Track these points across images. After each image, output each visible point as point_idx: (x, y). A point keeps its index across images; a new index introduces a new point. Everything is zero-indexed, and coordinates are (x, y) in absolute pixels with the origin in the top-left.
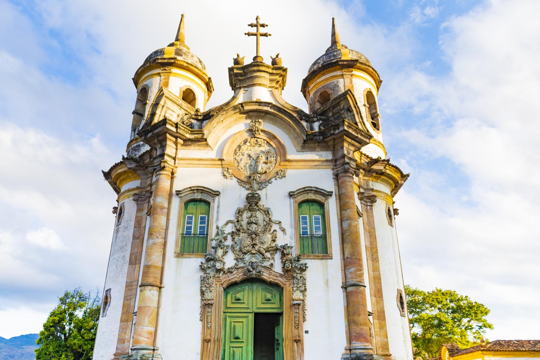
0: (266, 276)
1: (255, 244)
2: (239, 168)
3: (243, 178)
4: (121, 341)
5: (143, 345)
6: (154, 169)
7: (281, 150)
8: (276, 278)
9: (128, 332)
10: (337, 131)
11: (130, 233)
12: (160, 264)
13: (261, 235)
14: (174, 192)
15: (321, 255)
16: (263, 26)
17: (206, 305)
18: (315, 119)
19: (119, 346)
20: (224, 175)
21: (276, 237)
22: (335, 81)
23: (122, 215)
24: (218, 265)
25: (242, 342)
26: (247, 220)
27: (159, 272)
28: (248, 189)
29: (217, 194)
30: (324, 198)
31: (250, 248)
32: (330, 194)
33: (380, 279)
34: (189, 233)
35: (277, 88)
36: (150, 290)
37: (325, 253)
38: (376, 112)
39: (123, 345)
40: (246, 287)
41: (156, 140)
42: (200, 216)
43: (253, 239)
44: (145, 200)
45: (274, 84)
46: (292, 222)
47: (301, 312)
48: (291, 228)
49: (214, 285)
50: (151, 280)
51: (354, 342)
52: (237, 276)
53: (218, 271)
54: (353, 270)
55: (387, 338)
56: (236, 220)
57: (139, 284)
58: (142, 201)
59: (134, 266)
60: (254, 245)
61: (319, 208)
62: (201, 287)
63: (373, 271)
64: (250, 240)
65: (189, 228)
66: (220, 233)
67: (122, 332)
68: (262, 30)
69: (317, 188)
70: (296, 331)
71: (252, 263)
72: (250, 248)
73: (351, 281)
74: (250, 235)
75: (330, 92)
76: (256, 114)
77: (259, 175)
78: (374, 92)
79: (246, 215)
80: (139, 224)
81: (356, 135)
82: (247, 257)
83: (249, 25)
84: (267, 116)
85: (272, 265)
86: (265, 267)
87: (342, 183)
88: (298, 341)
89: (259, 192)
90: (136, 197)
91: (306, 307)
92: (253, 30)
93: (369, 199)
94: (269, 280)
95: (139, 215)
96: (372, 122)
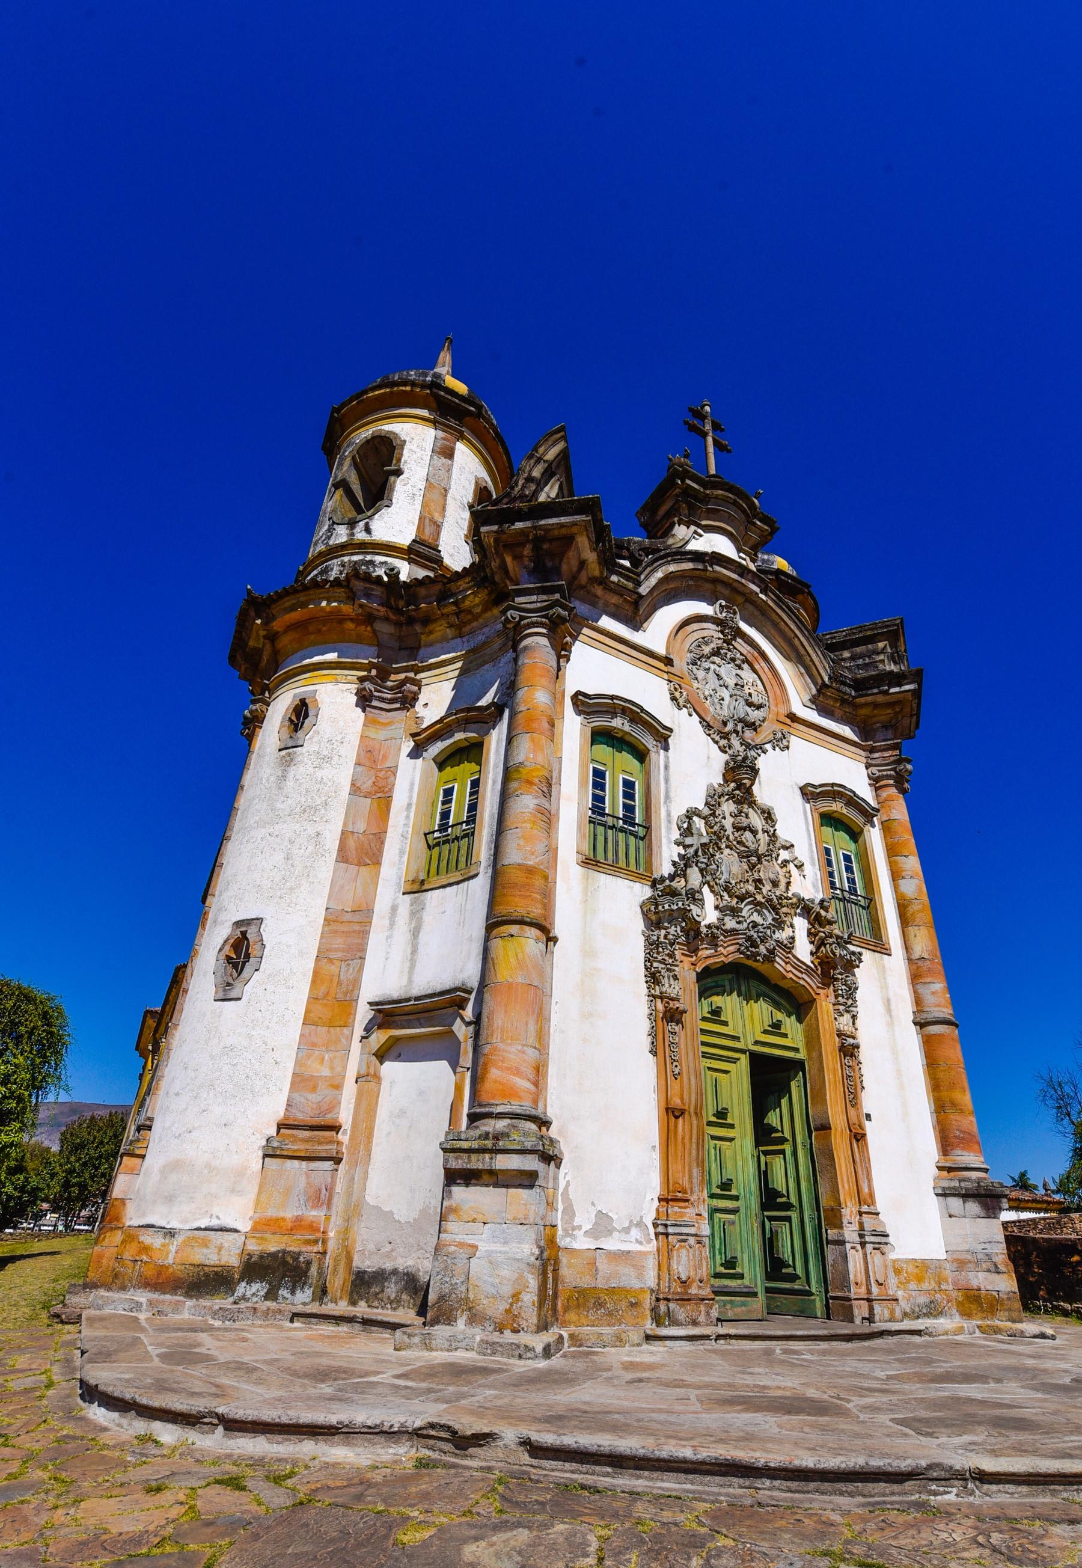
1: (760, 881)
6: (522, 618)
7: (777, 689)
8: (799, 974)
10: (892, 690)
11: (342, 774)
20: (674, 699)
25: (732, 1126)
26: (732, 820)
31: (751, 888)
39: (310, 1096)
41: (527, 551)
43: (752, 867)
44: (392, 701)
47: (857, 1068)
48: (813, 864)
51: (959, 1152)
59: (353, 869)
62: (649, 960)
67: (309, 1056)
72: (751, 888)
84: (747, 605)
90: (368, 685)
95: (372, 735)
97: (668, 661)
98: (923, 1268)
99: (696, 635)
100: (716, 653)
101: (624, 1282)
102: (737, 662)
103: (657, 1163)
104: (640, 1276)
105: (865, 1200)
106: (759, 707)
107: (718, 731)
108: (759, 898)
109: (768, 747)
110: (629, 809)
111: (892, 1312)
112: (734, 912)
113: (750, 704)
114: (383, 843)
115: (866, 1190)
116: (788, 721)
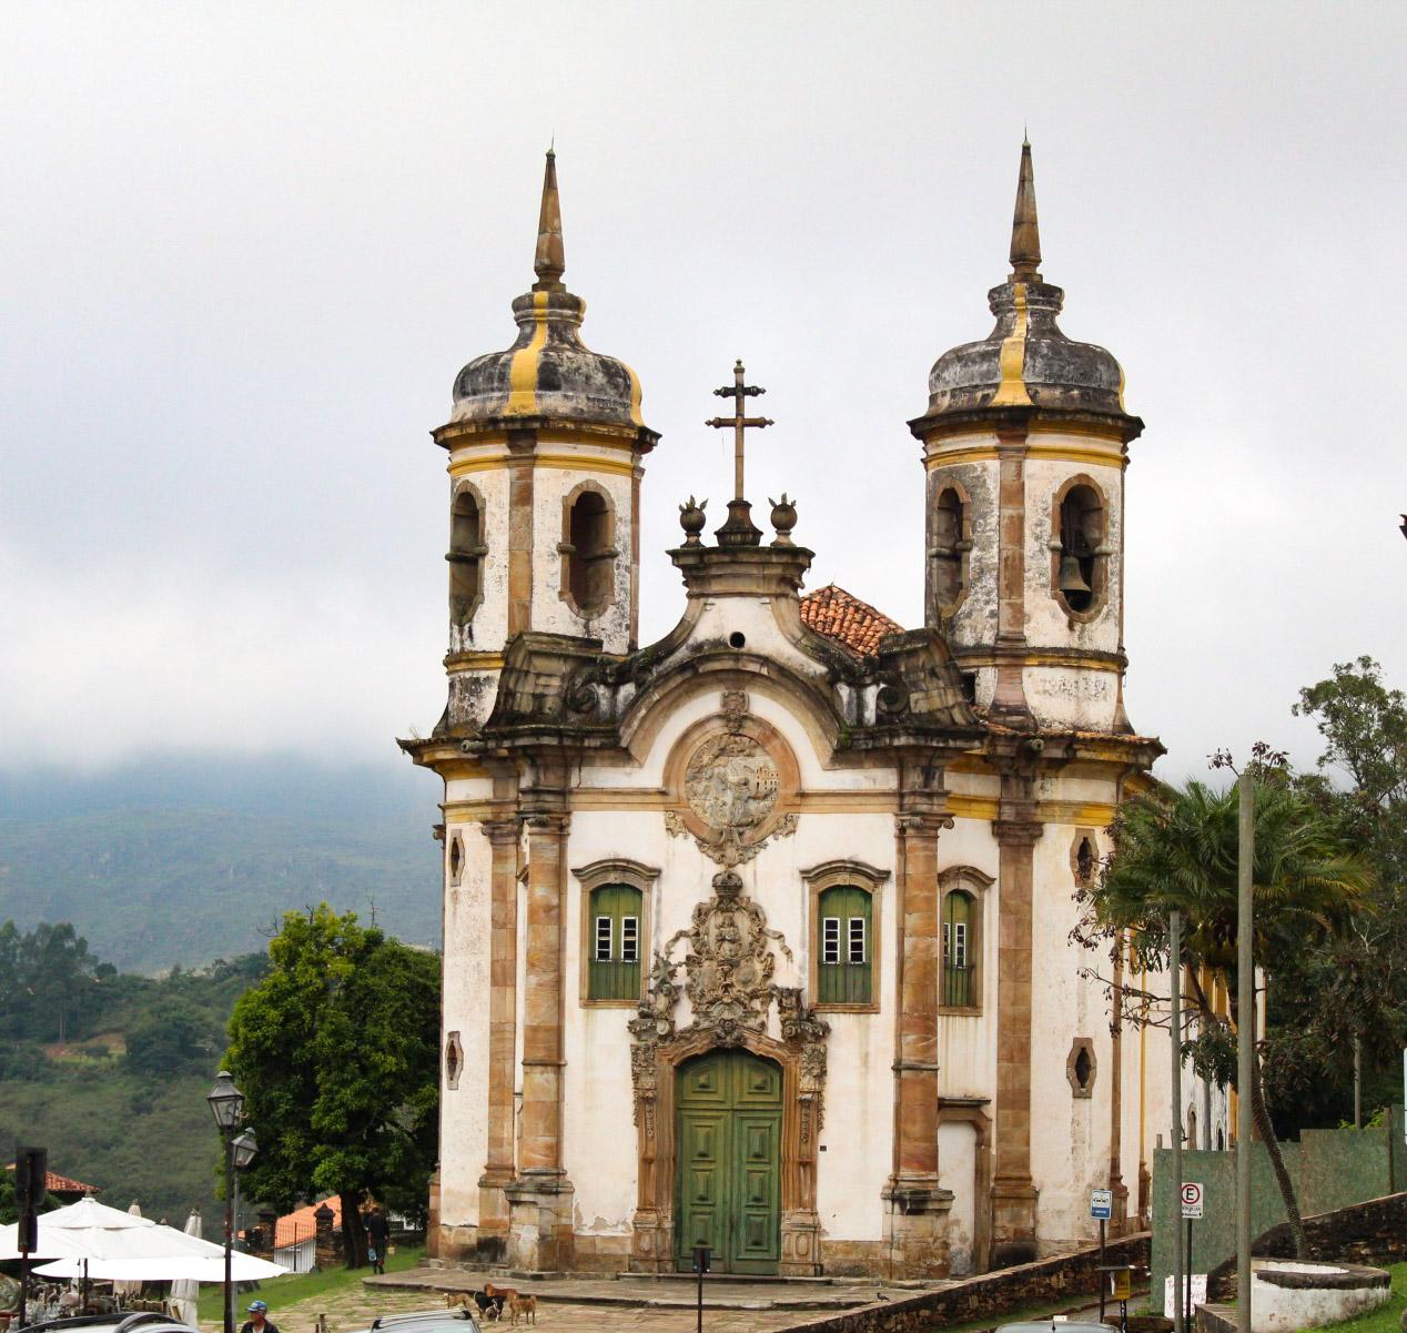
0: (751, 1045)
1: (731, 985)
2: (699, 811)
3: (705, 835)
4: (495, 1141)
5: (540, 1168)
9: (508, 1125)
11: (484, 910)
12: (555, 1024)
13: (743, 963)
14: (570, 873)
15: (857, 1005)
16: (755, 392)
17: (644, 1102)
18: (868, 681)
19: (493, 1152)
21: (772, 969)
22: (976, 462)
23: (460, 862)
24: (662, 1028)
27: (553, 1038)
28: (719, 862)
29: (654, 874)
30: (871, 884)
32: (883, 876)
33: (1027, 1021)
34: (604, 955)
35: (785, 596)
36: (542, 1073)
37: (865, 1003)
38: (1099, 542)
40: (720, 1063)
42: (624, 918)
43: (726, 975)
44: (509, 835)
45: (774, 589)
46: (803, 933)
48: (803, 946)
49: (656, 1062)
50: (541, 1055)
52: (699, 1045)
53: (663, 1038)
54: (911, 1038)
55: (1028, 1144)
56: (693, 932)
57: (520, 1057)
58: (502, 835)
60: (727, 987)
61: (861, 900)
63: (1013, 1004)
64: (719, 975)
65: (604, 944)
66: (661, 965)
68: (753, 408)
69: (857, 864)
70: (804, 1147)
71: (725, 1021)
72: (720, 992)
73: (908, 1059)
74: (721, 963)
75: (964, 498)
76: (731, 676)
77: (741, 830)
78: (1102, 474)
79: (715, 921)
80: (501, 893)
81: (941, 745)
82: (715, 1011)
83: (718, 393)
85: (763, 1025)
86: (750, 1029)
87: (914, 849)
88: (809, 1165)
89: (740, 870)
91: (825, 1105)
92: (727, 408)
93: (1017, 836)
94: (758, 1053)
95: (500, 871)
96: (1068, 593)
97: (663, 793)
98: (853, 1246)
99: (698, 744)
100: (723, 752)
101: (613, 1251)
102: (748, 751)
103: (636, 1191)
104: (623, 1249)
105: (810, 1207)
106: (765, 796)
107: (714, 844)
108: (725, 1000)
109: (770, 840)
110: (629, 945)
111: (806, 1271)
112: (707, 1014)
113: (755, 798)
114: (515, 968)
115: (806, 1197)
116: (797, 800)
